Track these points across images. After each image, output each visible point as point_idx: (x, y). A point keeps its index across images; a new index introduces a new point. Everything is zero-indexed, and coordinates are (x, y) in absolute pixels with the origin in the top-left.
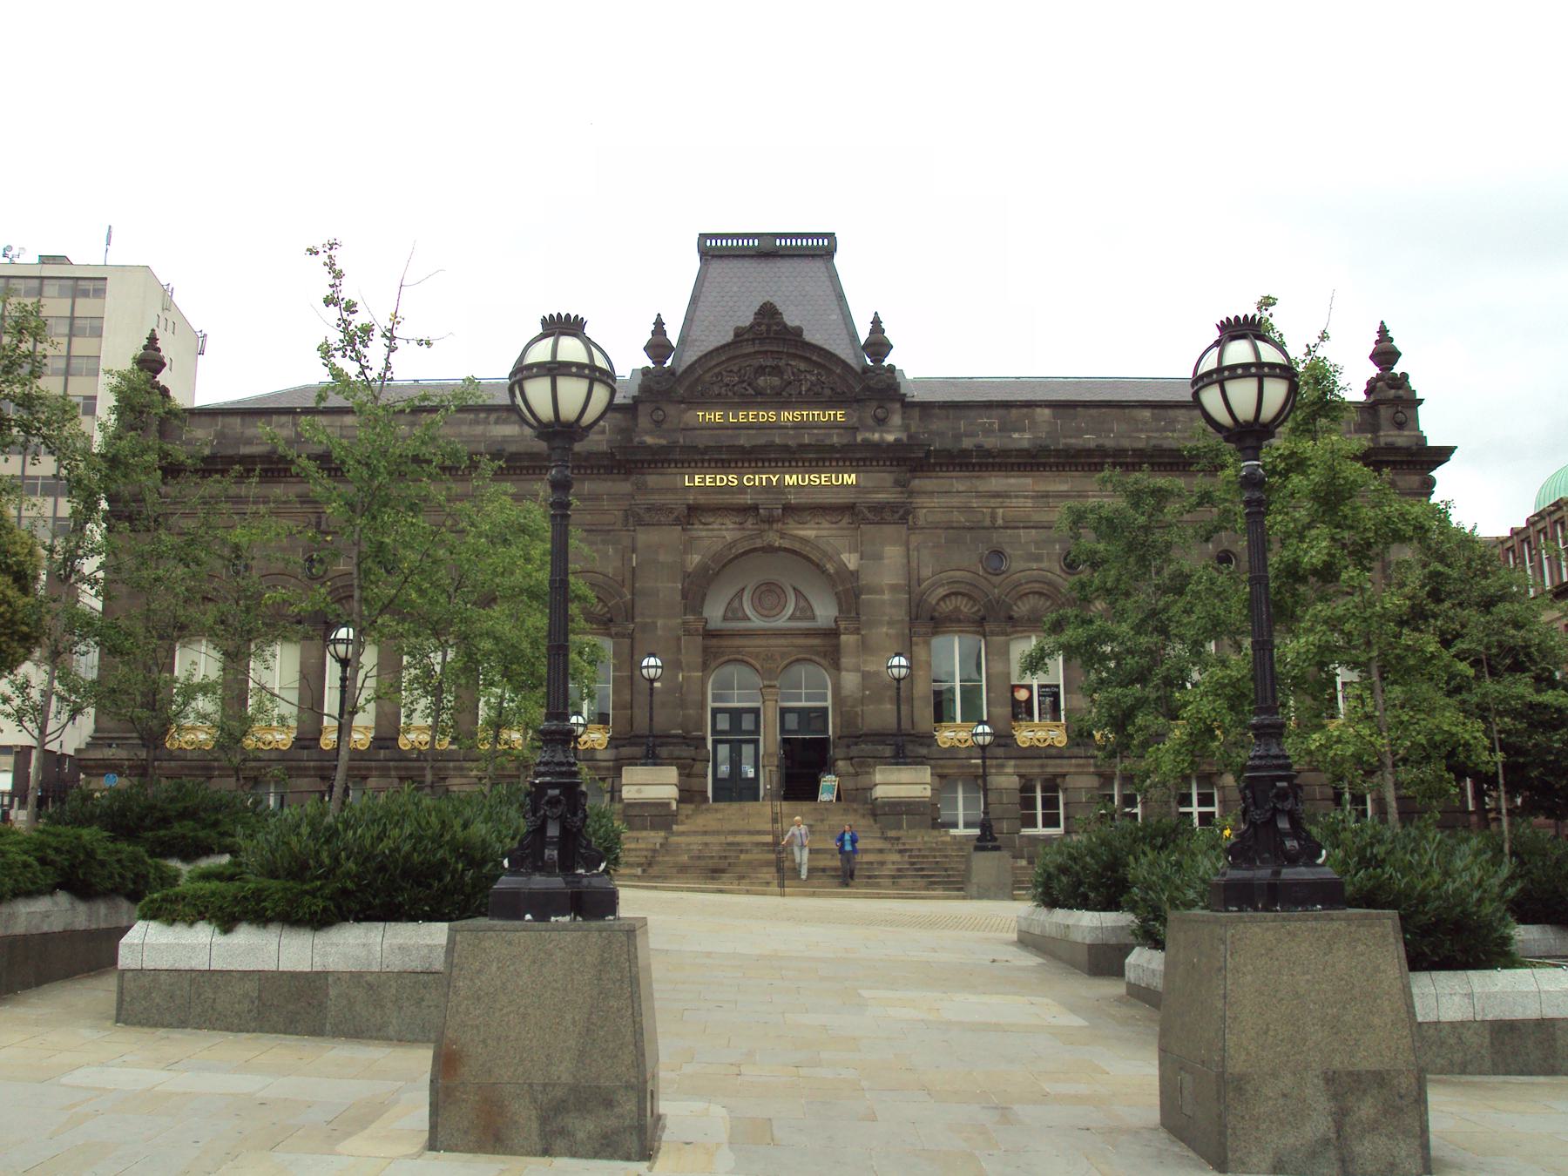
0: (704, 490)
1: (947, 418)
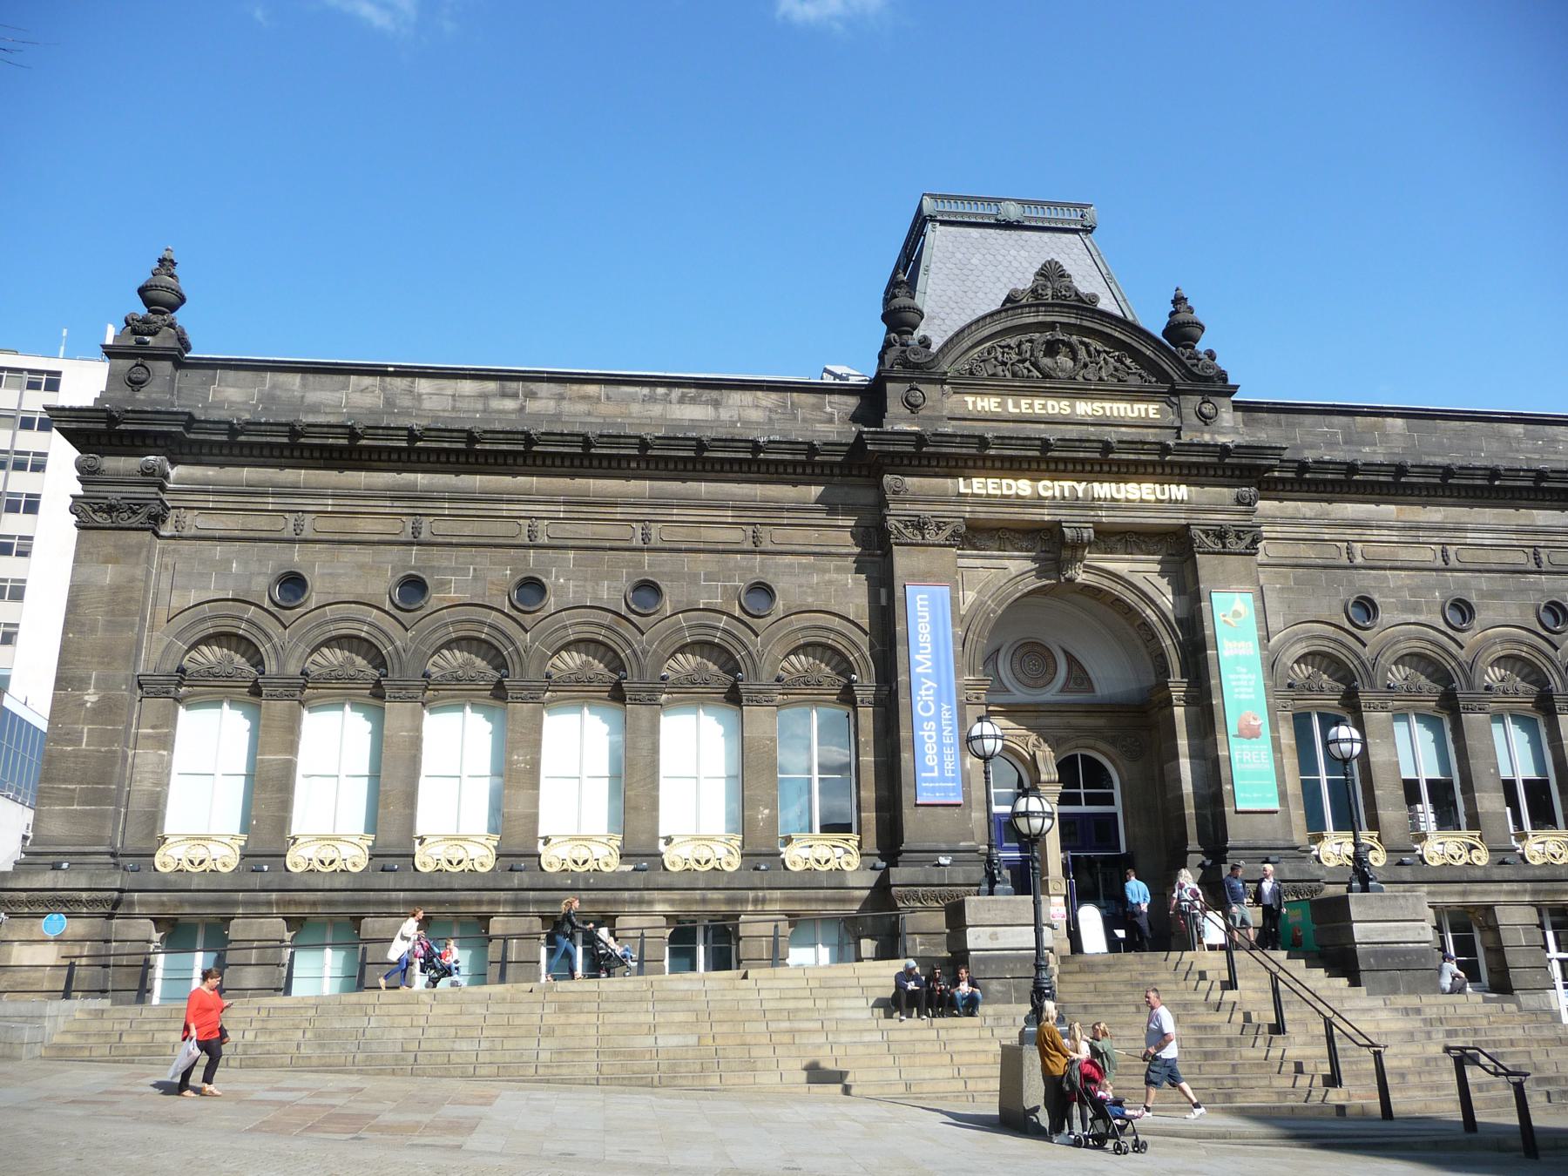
0: (988, 501)
1: (1279, 424)
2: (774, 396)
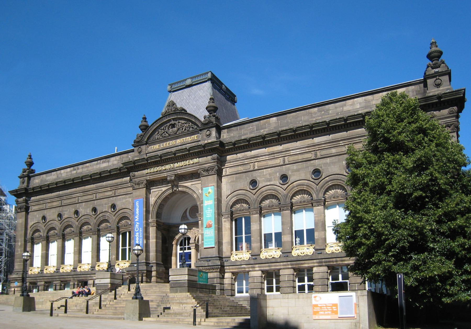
2: (119, 156)
